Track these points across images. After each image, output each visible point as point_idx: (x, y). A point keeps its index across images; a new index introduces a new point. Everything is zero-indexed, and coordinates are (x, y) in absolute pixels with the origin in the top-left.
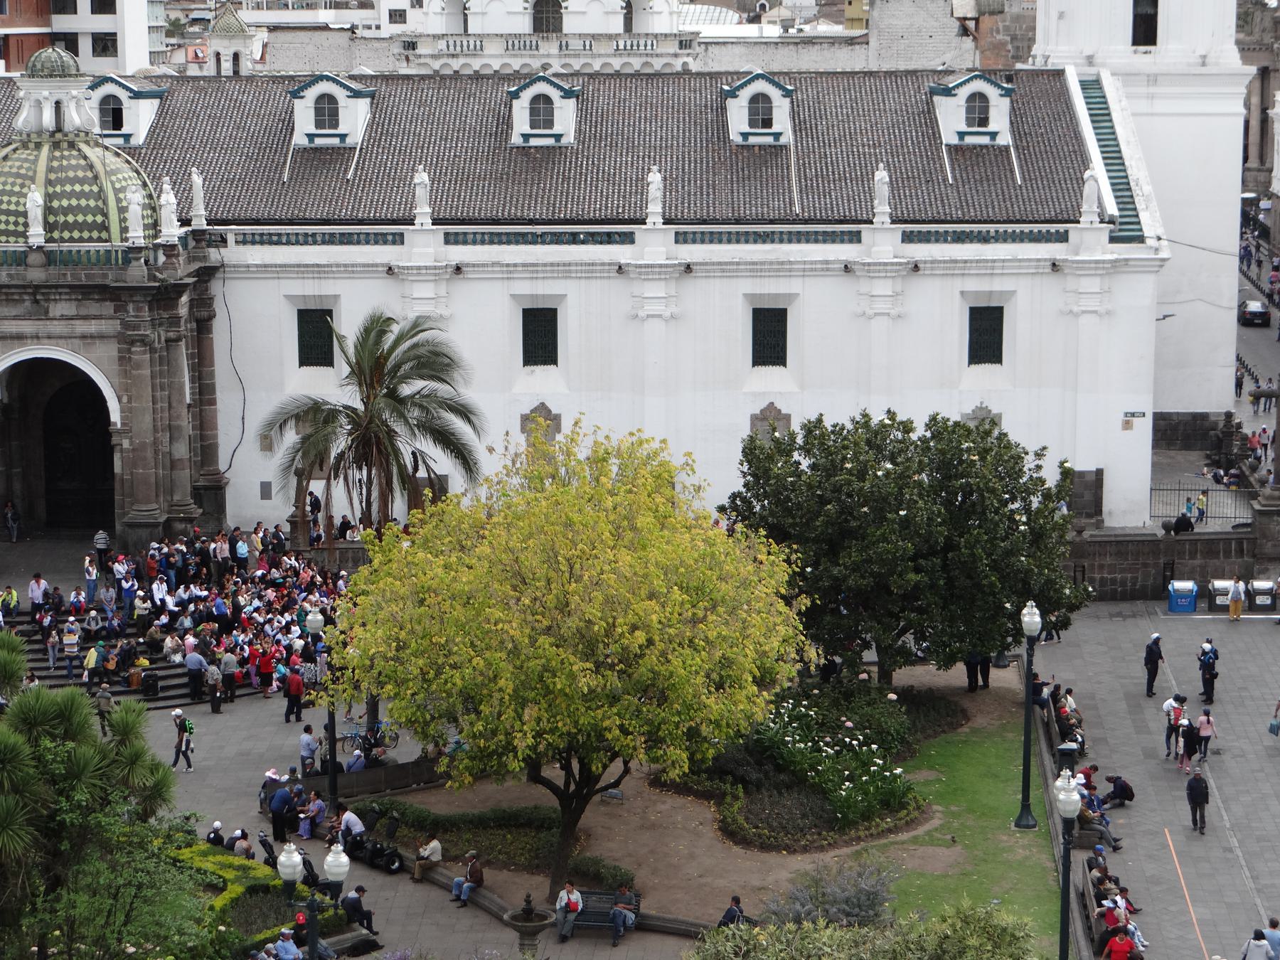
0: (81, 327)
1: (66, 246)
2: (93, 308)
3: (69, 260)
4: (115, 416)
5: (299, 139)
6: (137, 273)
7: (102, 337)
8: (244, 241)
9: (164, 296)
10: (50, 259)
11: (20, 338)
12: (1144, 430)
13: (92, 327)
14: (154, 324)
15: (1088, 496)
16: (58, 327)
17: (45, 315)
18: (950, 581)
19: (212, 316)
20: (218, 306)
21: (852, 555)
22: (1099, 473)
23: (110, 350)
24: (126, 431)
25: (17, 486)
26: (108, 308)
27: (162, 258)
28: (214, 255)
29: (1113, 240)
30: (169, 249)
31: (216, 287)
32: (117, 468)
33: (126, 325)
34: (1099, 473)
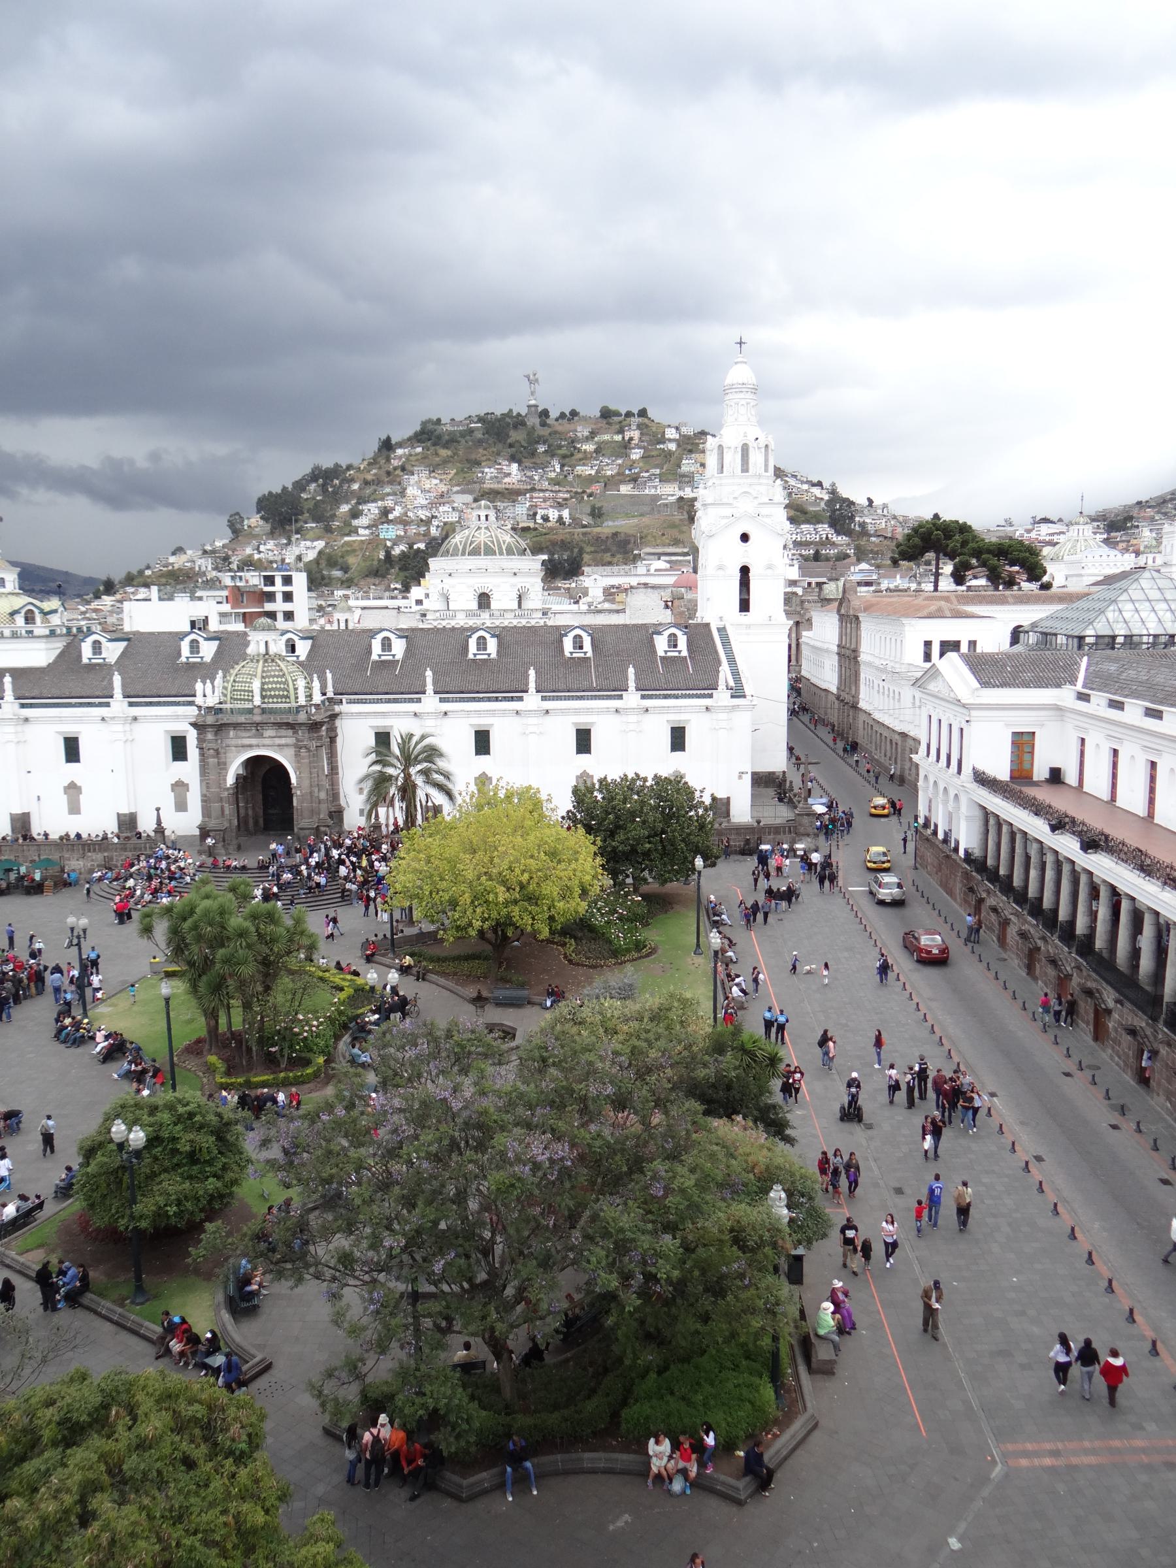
0: (278, 741)
1: (270, 706)
2: (283, 732)
3: (272, 711)
4: (294, 780)
5: (374, 657)
6: (302, 717)
7: (287, 745)
8: (350, 702)
9: (314, 726)
10: (263, 711)
11: (250, 746)
12: (748, 779)
13: (283, 741)
14: (311, 739)
15: (724, 809)
16: (267, 741)
17: (261, 736)
18: (664, 847)
19: (336, 736)
20: (339, 731)
21: (621, 836)
22: (728, 798)
23: (291, 752)
24: (299, 786)
25: (250, 812)
26: (290, 732)
27: (314, 710)
28: (337, 708)
29: (732, 697)
30: (317, 706)
31: (338, 723)
32: (295, 804)
33: (298, 740)
34: (728, 798)
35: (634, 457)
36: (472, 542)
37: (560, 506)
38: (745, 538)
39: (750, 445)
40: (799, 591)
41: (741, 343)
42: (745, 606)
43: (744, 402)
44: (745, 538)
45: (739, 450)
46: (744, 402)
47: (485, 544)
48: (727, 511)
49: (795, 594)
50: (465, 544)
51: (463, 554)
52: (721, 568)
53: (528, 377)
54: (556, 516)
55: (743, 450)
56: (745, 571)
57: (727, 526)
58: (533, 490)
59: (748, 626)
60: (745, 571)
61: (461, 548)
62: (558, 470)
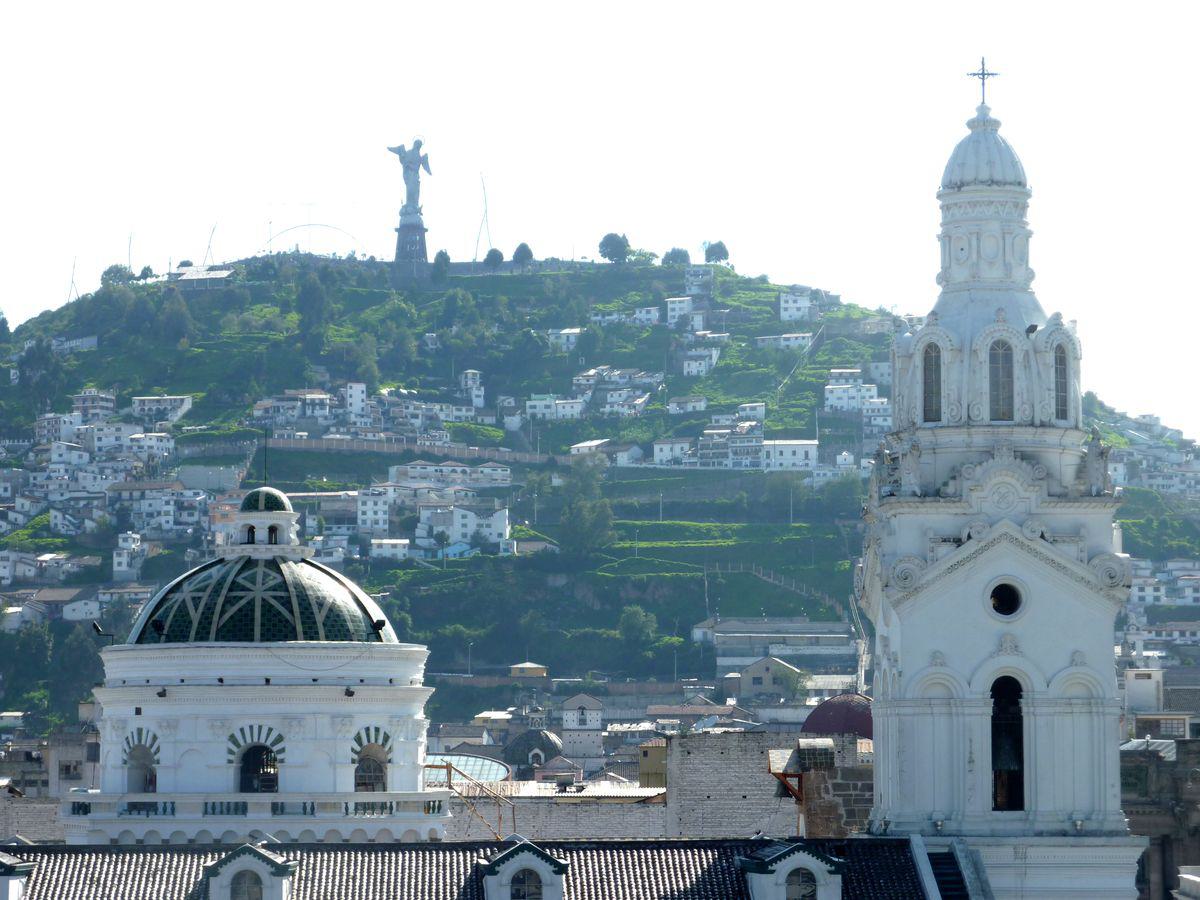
36: (229, 601)
37: (484, 501)
38: (1006, 599)
39: (1014, 342)
40: (1168, 751)
41: (983, 75)
42: (1010, 791)
44: (1006, 599)
47: (267, 607)
49: (1153, 756)
50: (210, 609)
51: (202, 636)
53: (399, 150)
54: (471, 529)
55: (993, 358)
56: (1007, 693)
58: (407, 457)
60: (1007, 693)
61: (195, 616)
62: (479, 402)
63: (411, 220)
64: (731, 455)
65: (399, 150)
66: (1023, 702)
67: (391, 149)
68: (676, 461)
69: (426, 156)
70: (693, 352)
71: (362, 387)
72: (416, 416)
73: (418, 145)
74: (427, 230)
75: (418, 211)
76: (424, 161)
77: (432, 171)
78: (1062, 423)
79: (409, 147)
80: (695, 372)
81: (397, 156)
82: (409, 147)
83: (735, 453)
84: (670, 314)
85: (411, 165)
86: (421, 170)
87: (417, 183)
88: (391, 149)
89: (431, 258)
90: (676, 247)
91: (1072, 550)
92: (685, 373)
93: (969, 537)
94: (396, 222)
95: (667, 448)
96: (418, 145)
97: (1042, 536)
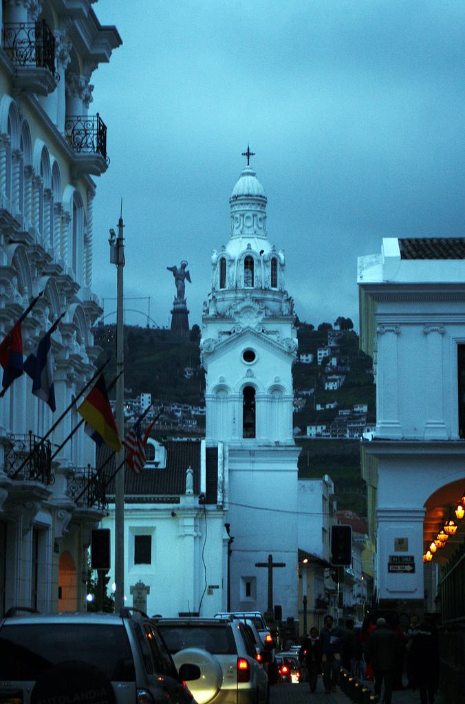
35: (330, 386)
38: (249, 356)
39: (254, 257)
41: (248, 154)
43: (250, 214)
44: (249, 356)
45: (243, 262)
46: (250, 214)
48: (228, 327)
52: (221, 388)
53: (173, 269)
56: (249, 393)
57: (228, 343)
59: (252, 453)
60: (249, 393)
63: (181, 306)
64: (348, 431)
65: (173, 269)
66: (255, 396)
67: (169, 269)
68: (318, 435)
69: (188, 272)
70: (329, 378)
71: (150, 395)
72: (178, 411)
73: (184, 266)
74: (188, 312)
75: (184, 303)
76: (187, 275)
77: (191, 280)
78: (274, 289)
79: (179, 267)
80: (331, 388)
81: (172, 273)
82: (179, 267)
83: (350, 430)
84: (319, 356)
85: (181, 277)
86: (186, 281)
87: (183, 287)
88: (169, 269)
89: (191, 328)
90: (325, 322)
91: (273, 337)
92: (326, 388)
93: (234, 332)
94: (172, 307)
95: (314, 428)
96: (184, 266)
97: (263, 331)
